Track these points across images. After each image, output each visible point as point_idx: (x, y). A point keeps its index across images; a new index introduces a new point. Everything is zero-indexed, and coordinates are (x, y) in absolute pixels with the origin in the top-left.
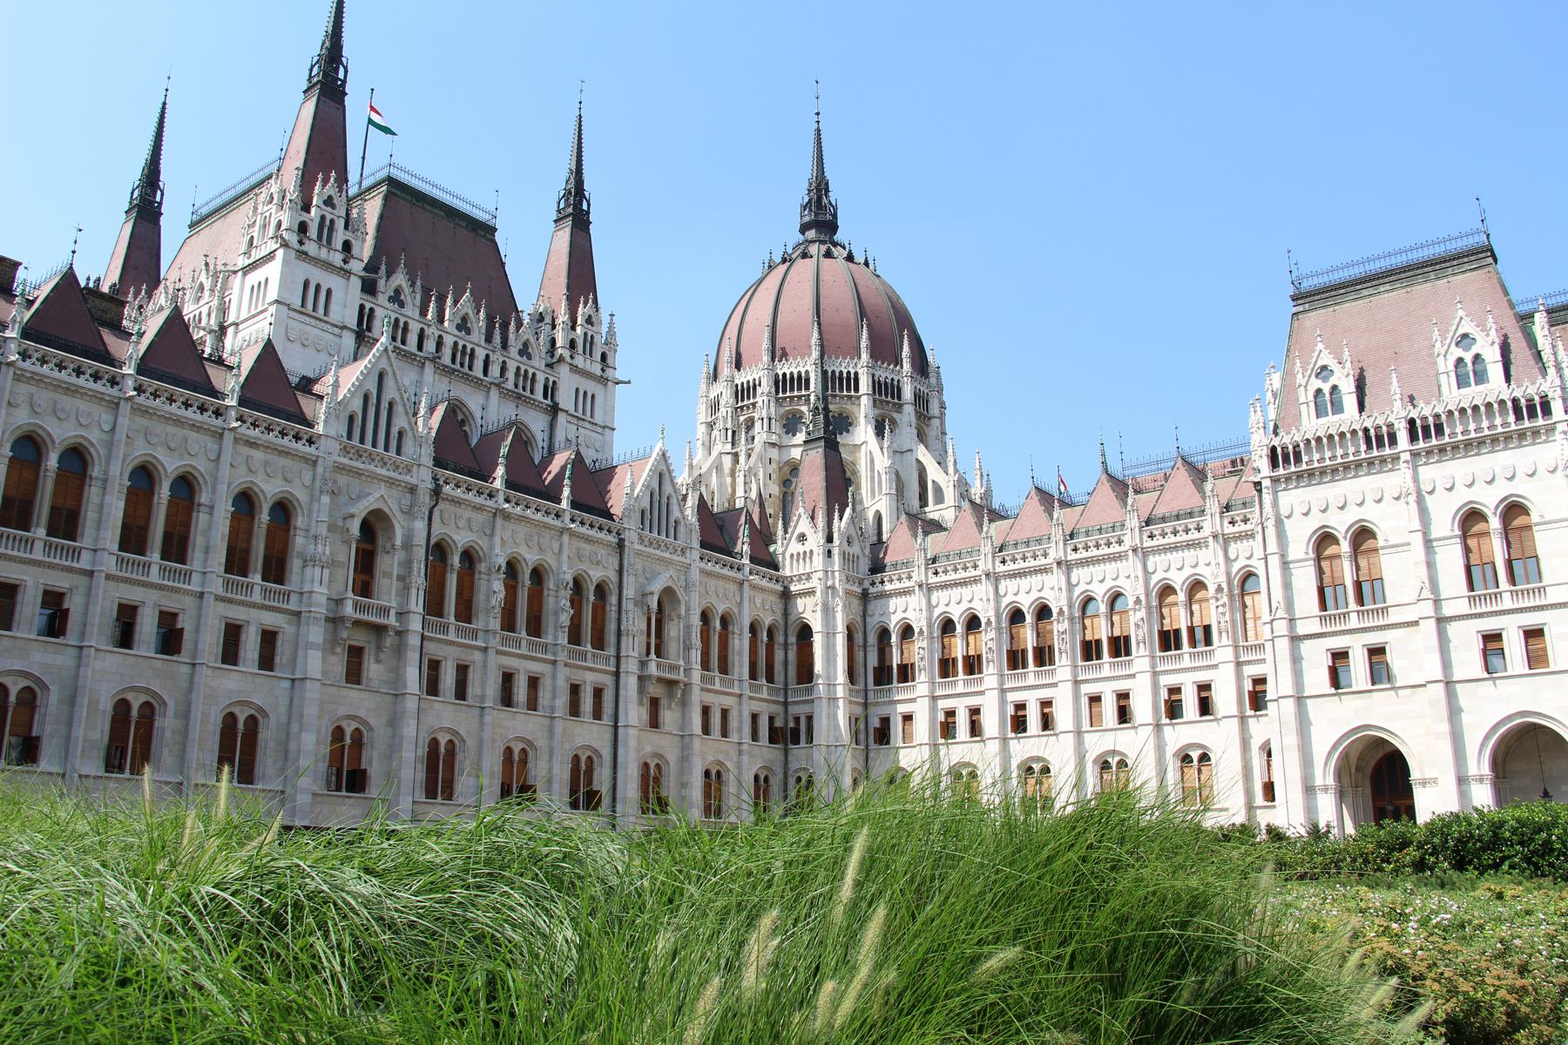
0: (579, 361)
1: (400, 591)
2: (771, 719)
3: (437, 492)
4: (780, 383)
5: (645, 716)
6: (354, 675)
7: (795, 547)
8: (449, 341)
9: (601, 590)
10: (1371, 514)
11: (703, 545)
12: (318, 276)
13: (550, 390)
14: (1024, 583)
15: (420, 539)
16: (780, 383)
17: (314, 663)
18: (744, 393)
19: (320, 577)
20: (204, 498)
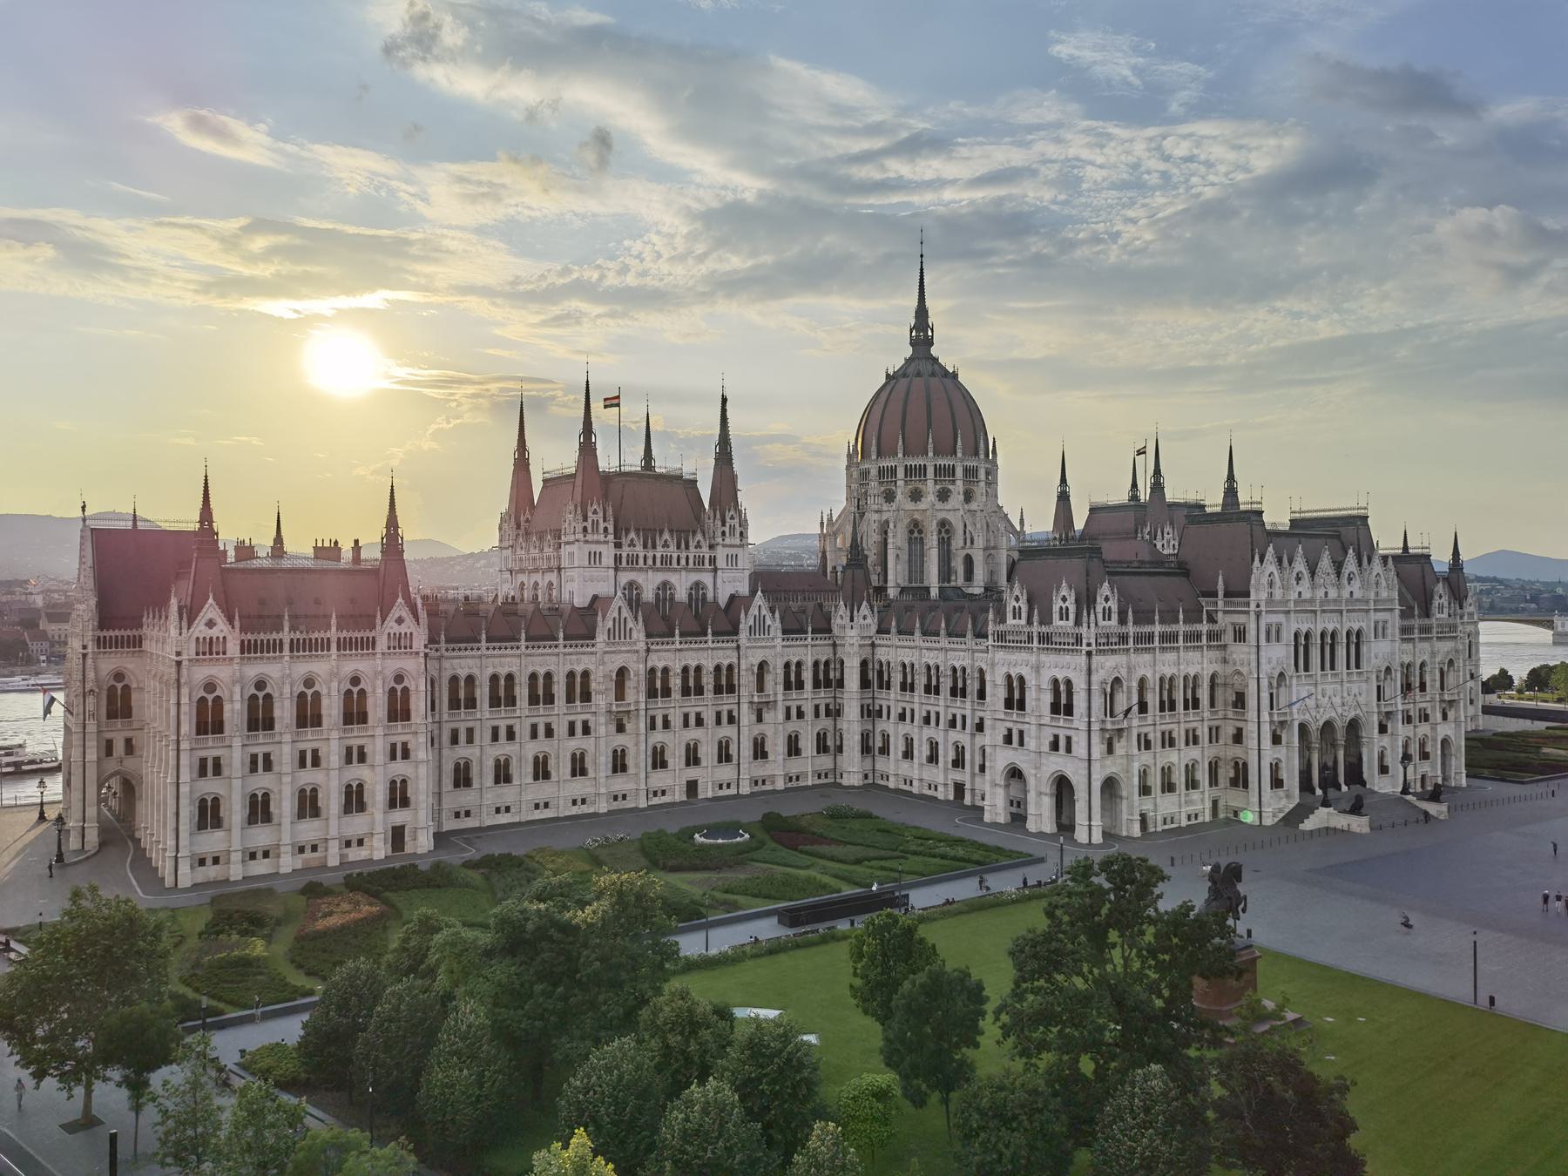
0: (728, 541)
1: (636, 693)
2: (827, 705)
3: (648, 650)
4: (882, 472)
5: (754, 717)
6: (620, 728)
7: (839, 621)
8: (658, 555)
9: (730, 667)
10: (1025, 672)
11: (784, 632)
12: (594, 548)
13: (713, 560)
14: (932, 654)
15: (642, 672)
16: (882, 472)
17: (602, 730)
18: (865, 474)
19: (602, 699)
20: (555, 679)
